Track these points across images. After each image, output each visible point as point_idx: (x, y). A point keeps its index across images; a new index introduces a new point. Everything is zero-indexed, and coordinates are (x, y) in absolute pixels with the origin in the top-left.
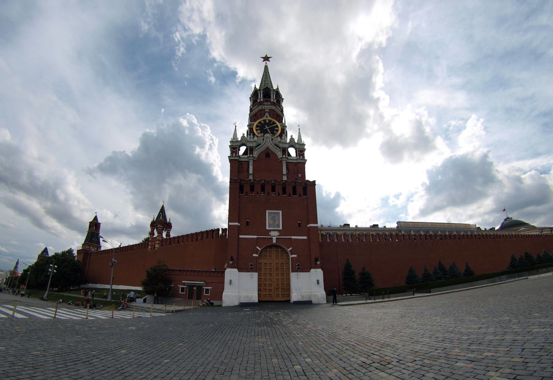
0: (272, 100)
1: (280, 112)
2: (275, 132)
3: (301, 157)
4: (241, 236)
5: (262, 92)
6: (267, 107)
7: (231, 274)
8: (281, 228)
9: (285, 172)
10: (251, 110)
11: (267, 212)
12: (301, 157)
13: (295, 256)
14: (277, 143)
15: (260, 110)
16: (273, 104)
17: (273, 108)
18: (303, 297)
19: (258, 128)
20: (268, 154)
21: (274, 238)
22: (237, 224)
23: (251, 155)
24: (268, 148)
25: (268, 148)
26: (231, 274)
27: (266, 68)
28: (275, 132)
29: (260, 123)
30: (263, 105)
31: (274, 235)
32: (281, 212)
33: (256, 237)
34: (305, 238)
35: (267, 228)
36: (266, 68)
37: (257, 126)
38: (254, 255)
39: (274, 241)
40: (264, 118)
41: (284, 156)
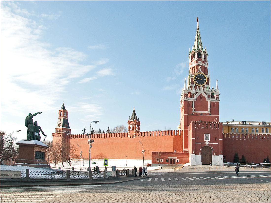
0: (202, 60)
1: (206, 66)
2: (204, 82)
3: (217, 99)
4: (196, 143)
5: (197, 54)
11: (205, 134)
12: (217, 99)
13: (214, 150)
14: (206, 92)
16: (203, 62)
17: (203, 64)
20: (201, 97)
23: (193, 98)
28: (204, 82)
29: (196, 76)
31: (207, 143)
33: (201, 143)
34: (218, 144)
35: (205, 140)
37: (195, 78)
41: (209, 99)
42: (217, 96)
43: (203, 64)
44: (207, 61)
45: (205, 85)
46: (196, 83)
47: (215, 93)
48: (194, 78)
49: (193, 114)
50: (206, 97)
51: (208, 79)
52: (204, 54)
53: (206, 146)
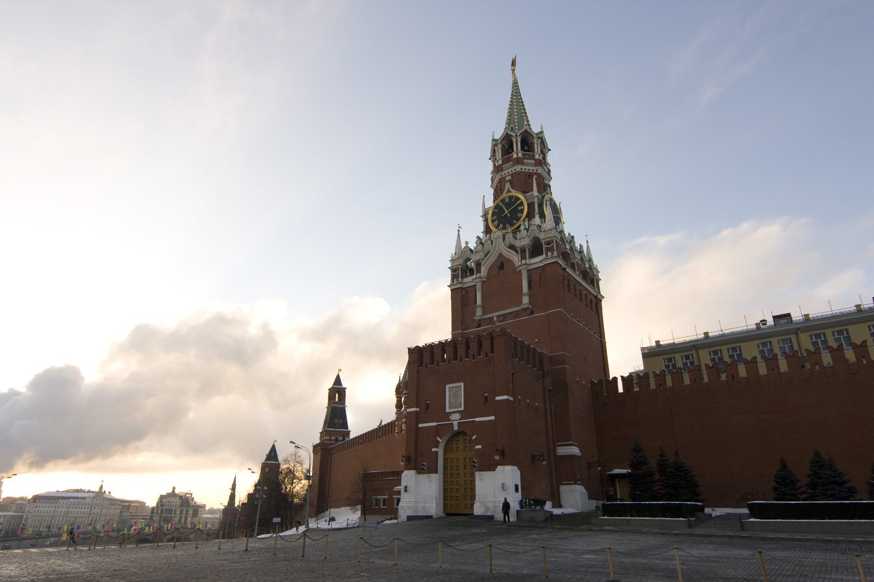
0: (515, 156)
1: (531, 168)
3: (549, 254)
4: (420, 425)
5: (500, 146)
6: (509, 170)
7: (409, 477)
8: (462, 409)
9: (525, 289)
10: (493, 181)
11: (447, 387)
15: (500, 181)
16: (518, 161)
17: (518, 168)
18: (487, 509)
19: (495, 217)
20: (502, 264)
21: (455, 423)
22: (414, 409)
24: (500, 255)
25: (500, 255)
26: (409, 477)
27: (515, 84)
30: (502, 170)
32: (462, 384)
33: (435, 424)
34: (492, 418)
35: (448, 410)
36: (515, 84)
38: (434, 450)
39: (456, 428)
40: (504, 195)
41: (524, 262)
42: (548, 243)
43: (518, 168)
44: (537, 157)
45: (520, 225)
46: (497, 227)
47: (542, 236)
48: (490, 215)
49: (479, 326)
50: (516, 258)
51: (531, 205)
52: (519, 140)
53: (458, 434)
